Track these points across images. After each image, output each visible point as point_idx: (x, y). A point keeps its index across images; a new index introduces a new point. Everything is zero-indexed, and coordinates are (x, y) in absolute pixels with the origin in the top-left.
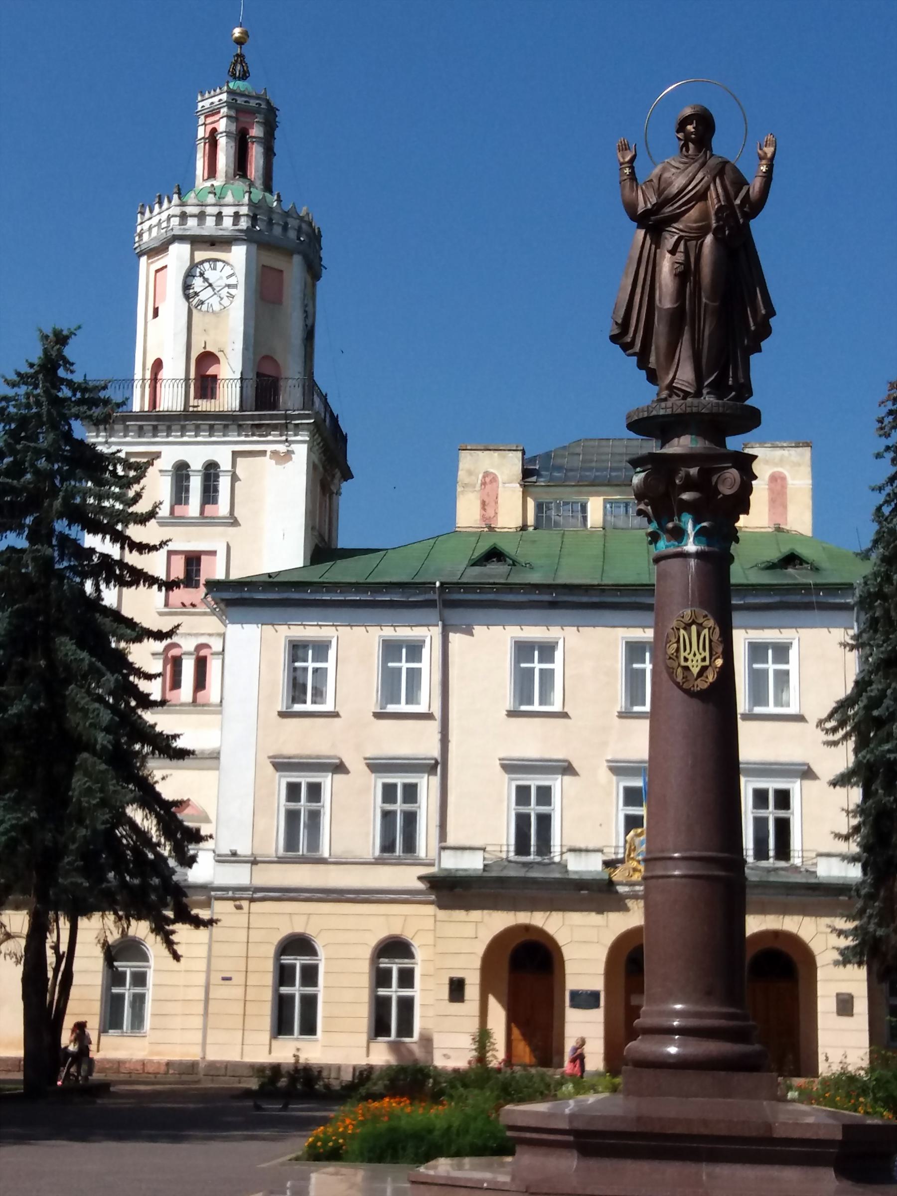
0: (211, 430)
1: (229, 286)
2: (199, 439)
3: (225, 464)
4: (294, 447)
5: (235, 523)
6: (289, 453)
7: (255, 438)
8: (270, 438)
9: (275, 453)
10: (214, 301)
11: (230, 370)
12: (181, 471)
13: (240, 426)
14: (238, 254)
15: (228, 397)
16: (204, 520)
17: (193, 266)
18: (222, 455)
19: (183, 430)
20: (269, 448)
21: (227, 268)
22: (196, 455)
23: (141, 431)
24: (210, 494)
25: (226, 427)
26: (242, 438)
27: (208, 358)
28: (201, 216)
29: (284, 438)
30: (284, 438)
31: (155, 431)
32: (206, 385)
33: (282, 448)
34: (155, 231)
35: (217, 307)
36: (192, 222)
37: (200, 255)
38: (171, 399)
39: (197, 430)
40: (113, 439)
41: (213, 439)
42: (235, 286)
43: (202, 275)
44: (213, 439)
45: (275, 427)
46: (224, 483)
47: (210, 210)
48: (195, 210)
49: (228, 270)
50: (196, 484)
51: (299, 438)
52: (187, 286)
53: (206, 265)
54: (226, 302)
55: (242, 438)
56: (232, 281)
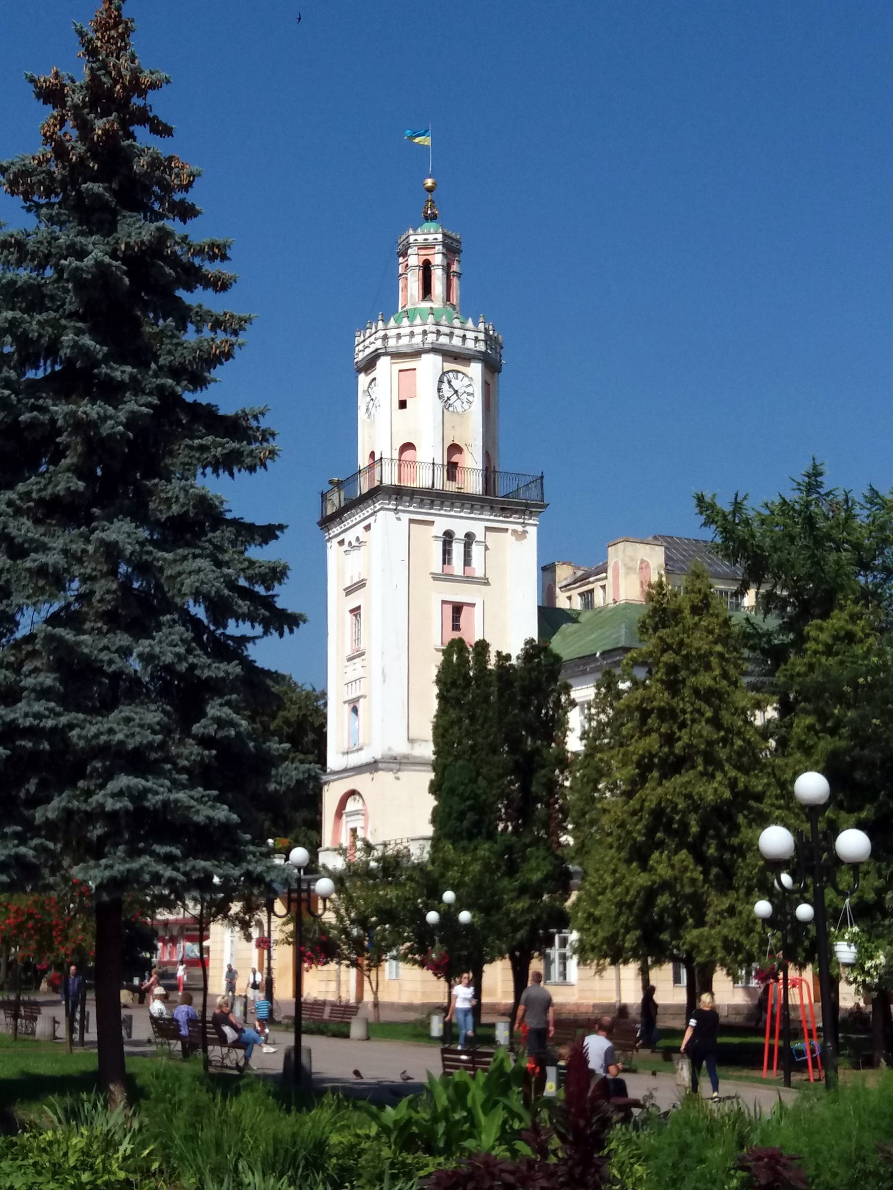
0: (472, 508)
1: (468, 394)
2: (462, 514)
3: (480, 537)
4: (528, 528)
5: (487, 583)
6: (525, 532)
7: (501, 518)
8: (511, 519)
9: (515, 532)
10: (458, 404)
11: (472, 460)
12: (448, 537)
13: (492, 508)
14: (476, 369)
15: (473, 484)
16: (469, 579)
17: (444, 374)
18: (478, 528)
19: (452, 506)
20: (511, 527)
21: (466, 379)
22: (461, 525)
23: (421, 504)
24: (467, 561)
25: (482, 507)
26: (492, 518)
27: (455, 449)
28: (451, 335)
29: (521, 521)
30: (521, 521)
31: (432, 504)
32: (452, 469)
33: (519, 528)
34: (405, 341)
35: (460, 410)
36: (431, 338)
37: (449, 366)
38: (422, 479)
39: (462, 507)
40: (400, 508)
41: (472, 516)
42: (472, 395)
43: (449, 382)
44: (472, 516)
45: (516, 512)
46: (477, 551)
47: (457, 332)
48: (446, 330)
49: (466, 381)
50: (458, 549)
51: (531, 522)
52: (439, 390)
53: (451, 374)
54: (466, 406)
55: (492, 518)
56: (469, 390)
